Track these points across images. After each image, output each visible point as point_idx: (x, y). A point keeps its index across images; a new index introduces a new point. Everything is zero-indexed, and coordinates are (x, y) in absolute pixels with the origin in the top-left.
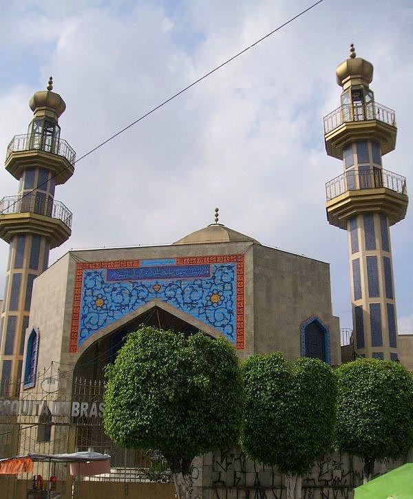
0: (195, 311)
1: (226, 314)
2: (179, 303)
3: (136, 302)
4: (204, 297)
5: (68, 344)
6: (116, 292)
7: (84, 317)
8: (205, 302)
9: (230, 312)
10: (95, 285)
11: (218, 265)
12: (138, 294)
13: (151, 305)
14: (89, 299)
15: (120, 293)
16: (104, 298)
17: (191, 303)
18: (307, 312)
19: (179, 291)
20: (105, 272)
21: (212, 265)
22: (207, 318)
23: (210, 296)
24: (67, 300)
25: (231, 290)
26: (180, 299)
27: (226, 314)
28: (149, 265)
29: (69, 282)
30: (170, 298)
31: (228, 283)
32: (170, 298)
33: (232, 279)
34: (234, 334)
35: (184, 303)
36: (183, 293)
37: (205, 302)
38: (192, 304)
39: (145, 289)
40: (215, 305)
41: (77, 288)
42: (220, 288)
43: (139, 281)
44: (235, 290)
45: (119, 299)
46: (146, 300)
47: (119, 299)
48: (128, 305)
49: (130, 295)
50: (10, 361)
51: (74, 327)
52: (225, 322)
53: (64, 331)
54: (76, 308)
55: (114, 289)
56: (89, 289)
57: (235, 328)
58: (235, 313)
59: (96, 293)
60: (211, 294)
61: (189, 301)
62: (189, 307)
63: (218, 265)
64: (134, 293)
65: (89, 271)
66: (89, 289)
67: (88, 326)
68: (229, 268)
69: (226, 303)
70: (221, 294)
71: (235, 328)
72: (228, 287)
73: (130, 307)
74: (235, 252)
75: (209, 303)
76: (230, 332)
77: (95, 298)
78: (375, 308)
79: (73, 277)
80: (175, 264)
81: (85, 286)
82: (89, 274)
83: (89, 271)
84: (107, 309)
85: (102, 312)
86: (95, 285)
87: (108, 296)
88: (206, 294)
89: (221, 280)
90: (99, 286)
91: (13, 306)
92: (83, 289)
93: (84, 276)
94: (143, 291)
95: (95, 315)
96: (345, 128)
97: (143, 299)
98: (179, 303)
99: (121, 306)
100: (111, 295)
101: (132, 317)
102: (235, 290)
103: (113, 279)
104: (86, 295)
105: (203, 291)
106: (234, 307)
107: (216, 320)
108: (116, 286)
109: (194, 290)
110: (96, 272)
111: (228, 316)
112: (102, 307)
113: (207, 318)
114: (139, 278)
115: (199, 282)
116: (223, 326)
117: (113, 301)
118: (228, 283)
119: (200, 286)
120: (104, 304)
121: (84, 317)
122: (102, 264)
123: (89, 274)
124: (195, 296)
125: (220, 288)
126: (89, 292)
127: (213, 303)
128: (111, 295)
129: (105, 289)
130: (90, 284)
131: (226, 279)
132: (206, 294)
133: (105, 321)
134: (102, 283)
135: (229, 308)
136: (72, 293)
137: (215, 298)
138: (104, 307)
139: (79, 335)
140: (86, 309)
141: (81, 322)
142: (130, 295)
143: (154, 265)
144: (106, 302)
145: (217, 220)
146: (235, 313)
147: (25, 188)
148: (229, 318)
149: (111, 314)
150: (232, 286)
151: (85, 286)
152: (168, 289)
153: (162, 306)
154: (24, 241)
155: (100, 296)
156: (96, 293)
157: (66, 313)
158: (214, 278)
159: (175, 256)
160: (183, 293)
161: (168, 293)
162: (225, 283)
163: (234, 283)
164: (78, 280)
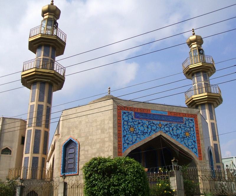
0: (179, 139)
1: (193, 142)
2: (171, 135)
3: (151, 131)
4: (182, 133)
5: (117, 151)
6: (140, 125)
7: (125, 136)
8: (183, 135)
9: (194, 142)
10: (129, 120)
11: (187, 118)
12: (151, 127)
13: (158, 134)
14: (126, 127)
15: (142, 125)
16: (134, 127)
17: (177, 135)
18: (209, 146)
19: (171, 129)
20: (133, 113)
21: (184, 118)
22: (185, 143)
23: (185, 133)
24: (114, 126)
25: (193, 131)
26: (172, 133)
27: (193, 142)
28: (155, 113)
29: (114, 115)
30: (167, 132)
31: (192, 127)
32: (167, 132)
33: (193, 126)
34: (197, 152)
35: (174, 135)
36: (173, 130)
37: (183, 135)
38: (177, 136)
39: (154, 125)
40: (187, 137)
41: (119, 120)
42: (189, 129)
43: (151, 121)
44: (195, 131)
45: (142, 128)
46: (156, 131)
47: (142, 128)
48: (147, 133)
49: (148, 128)
50: (37, 158)
51: (119, 141)
52: (193, 146)
53: (114, 143)
54: (119, 131)
55: (139, 123)
56: (125, 121)
57: (197, 149)
58: (196, 143)
59: (129, 124)
60: (185, 132)
61: (176, 134)
62: (176, 137)
63: (187, 118)
64: (149, 126)
65: (125, 111)
66: (125, 121)
67: (127, 142)
68: (192, 120)
69: (192, 137)
70: (189, 132)
71: (197, 149)
72: (192, 129)
73: (148, 134)
74: (193, 113)
75: (185, 136)
76: (195, 151)
77: (129, 127)
78: (216, 145)
79: (116, 113)
80: (167, 114)
81: (123, 119)
82: (125, 113)
83: (125, 111)
84: (136, 134)
85: (134, 135)
86: (129, 120)
87: (136, 126)
88: (183, 132)
89: (189, 126)
90: (131, 120)
91: (38, 124)
92: (122, 121)
93: (122, 114)
94: (153, 126)
95: (130, 136)
96: (201, 65)
97: (154, 130)
98: (171, 135)
99: (144, 133)
100: (138, 126)
101: (150, 139)
102: (195, 131)
103: (138, 118)
104: (124, 125)
105: (182, 130)
106: (196, 139)
107: (189, 145)
108: (140, 121)
109: (177, 129)
110: (128, 113)
111: (194, 143)
112: (133, 132)
113: (185, 143)
114: (151, 119)
115: (179, 125)
116: (192, 148)
117: (139, 130)
118: (192, 127)
119: (180, 127)
120: (135, 131)
121: (125, 136)
122: (131, 109)
123: (125, 113)
124: (179, 132)
125: (189, 129)
126: (125, 123)
127: (186, 136)
128: (138, 126)
129: (134, 122)
130: (126, 119)
131: (191, 125)
132: (183, 132)
133: (136, 140)
134: (132, 119)
135: (194, 139)
136: (116, 122)
137: (187, 134)
138: (135, 132)
139: (122, 146)
140: (125, 132)
141: (123, 139)
142: (148, 128)
143: (158, 113)
144: (135, 129)
145: (110, 93)
146: (196, 143)
147: (44, 56)
148: (194, 144)
149: (139, 136)
150: (193, 129)
151: (123, 119)
152: (166, 127)
153: (164, 135)
154: (45, 86)
155: (132, 126)
156: (129, 124)
157: (114, 133)
158: (185, 124)
159: (167, 110)
160: (173, 130)
161: (167, 129)
162: (191, 127)
163: (194, 127)
164: (119, 116)
